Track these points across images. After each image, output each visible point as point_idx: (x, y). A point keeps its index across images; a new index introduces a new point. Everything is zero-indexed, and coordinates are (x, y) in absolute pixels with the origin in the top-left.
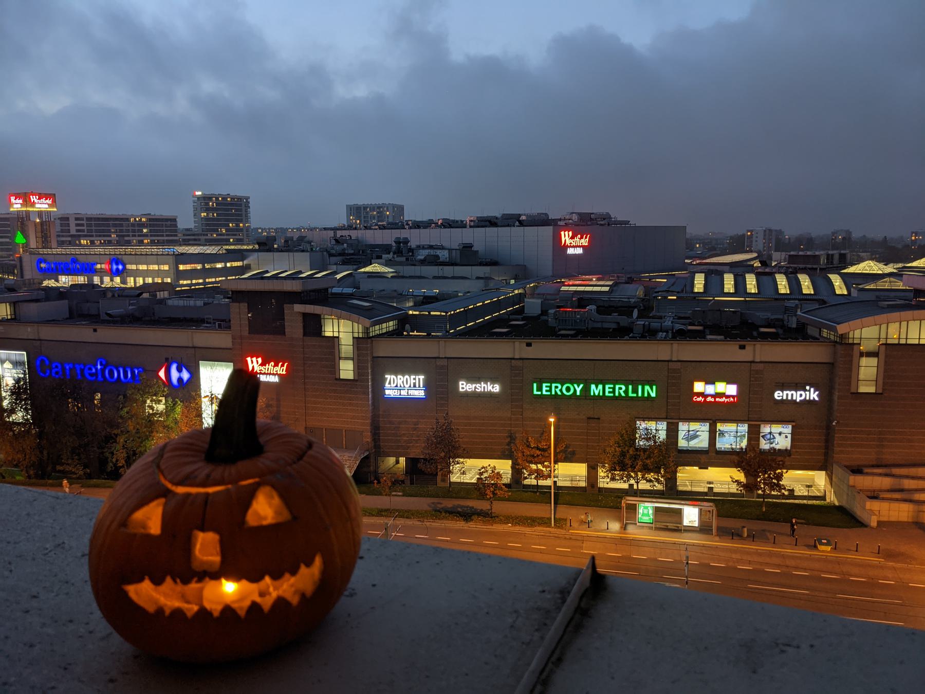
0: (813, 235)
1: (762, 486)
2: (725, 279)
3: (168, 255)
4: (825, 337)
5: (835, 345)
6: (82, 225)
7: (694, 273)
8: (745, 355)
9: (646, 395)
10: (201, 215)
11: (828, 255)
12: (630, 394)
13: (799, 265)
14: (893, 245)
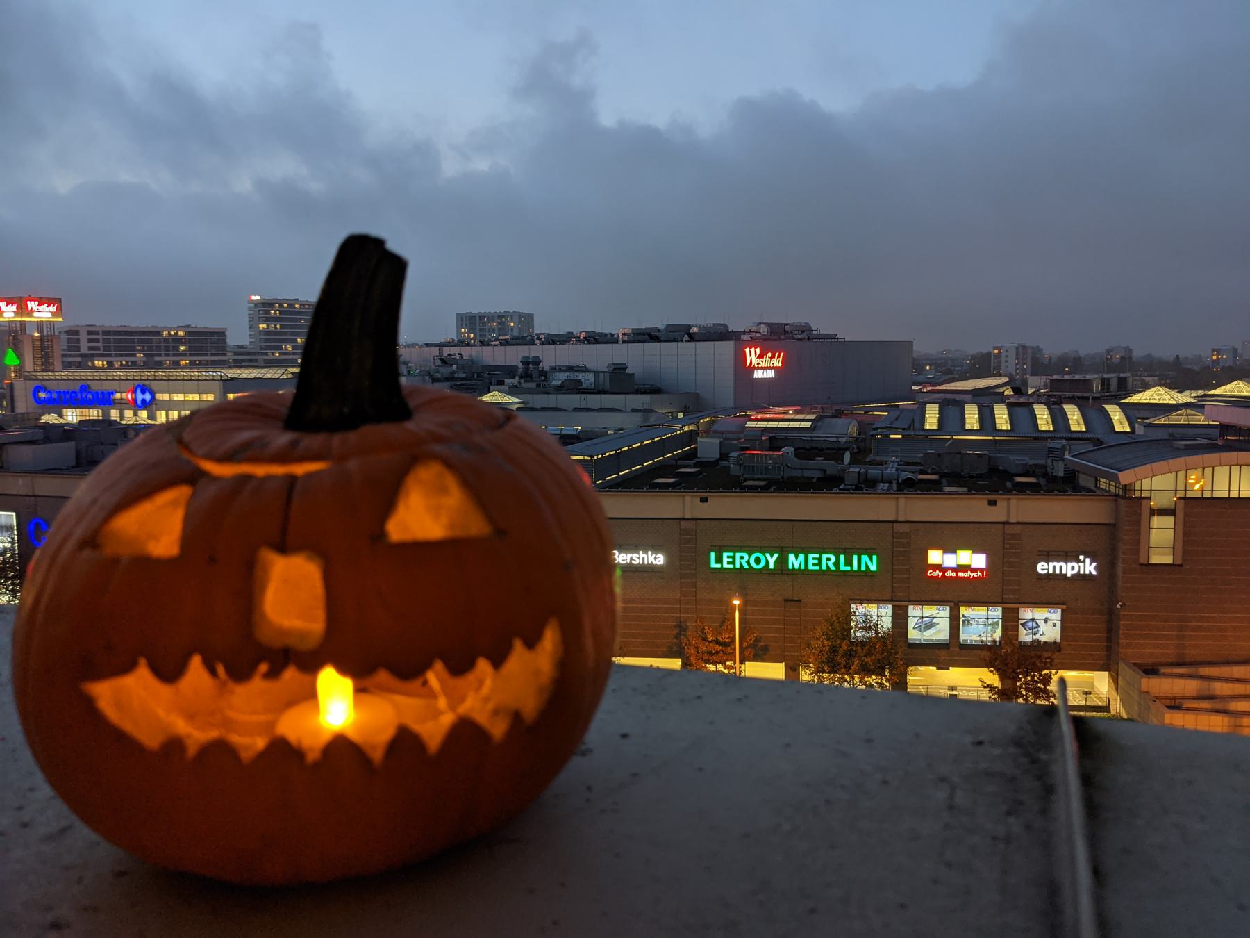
0: (1082, 353)
1: (1024, 693)
3: (213, 380)
5: (1116, 500)
6: (97, 341)
8: (997, 513)
9: (863, 568)
11: (1103, 380)
12: (843, 567)
14: (1189, 366)
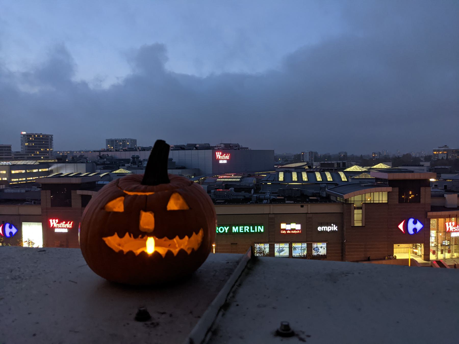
0: (331, 154)
2: (293, 175)
3: (6, 165)
5: (343, 205)
8: (303, 210)
9: (259, 231)
12: (252, 231)
13: (325, 168)
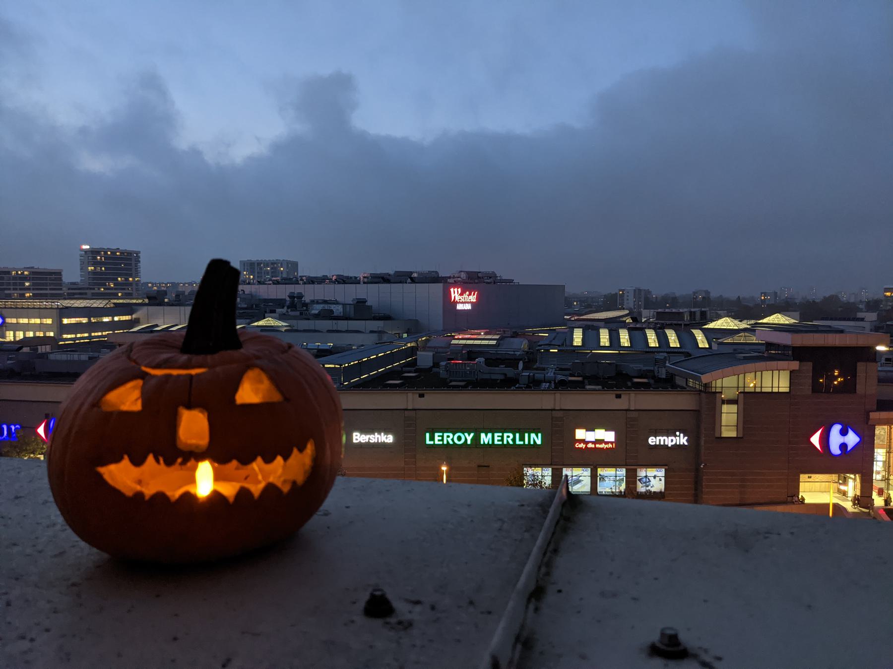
0: (677, 294)
2: (601, 334)
3: (51, 308)
4: (691, 387)
5: (700, 394)
7: (574, 328)
9: (532, 443)
10: (88, 269)
12: (518, 442)
